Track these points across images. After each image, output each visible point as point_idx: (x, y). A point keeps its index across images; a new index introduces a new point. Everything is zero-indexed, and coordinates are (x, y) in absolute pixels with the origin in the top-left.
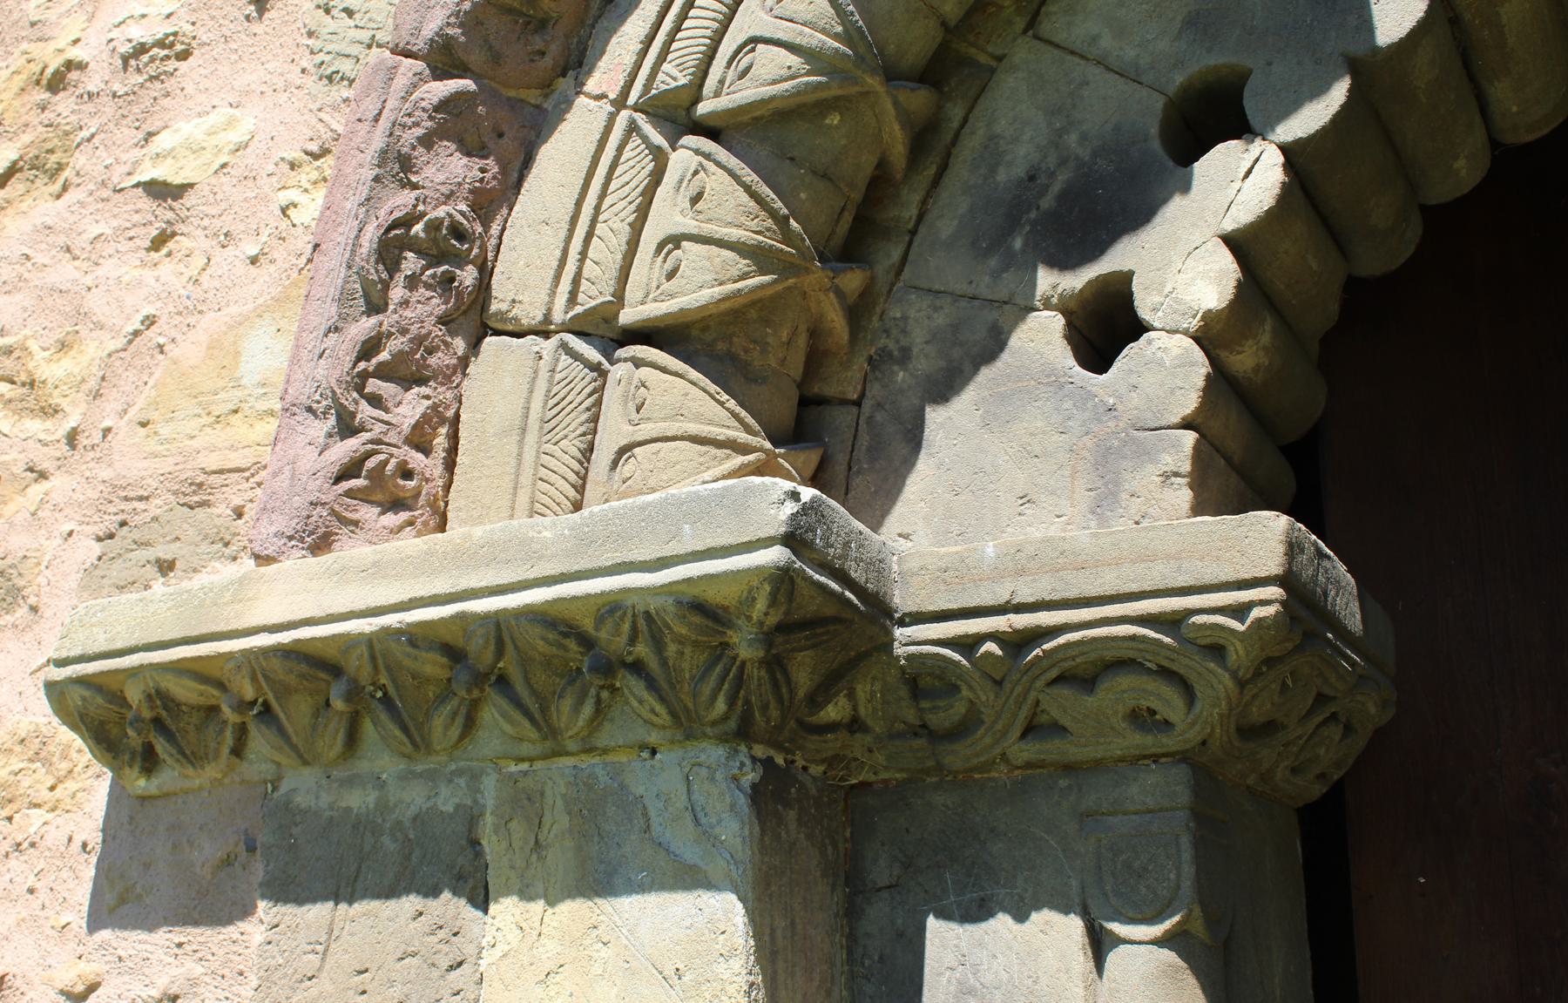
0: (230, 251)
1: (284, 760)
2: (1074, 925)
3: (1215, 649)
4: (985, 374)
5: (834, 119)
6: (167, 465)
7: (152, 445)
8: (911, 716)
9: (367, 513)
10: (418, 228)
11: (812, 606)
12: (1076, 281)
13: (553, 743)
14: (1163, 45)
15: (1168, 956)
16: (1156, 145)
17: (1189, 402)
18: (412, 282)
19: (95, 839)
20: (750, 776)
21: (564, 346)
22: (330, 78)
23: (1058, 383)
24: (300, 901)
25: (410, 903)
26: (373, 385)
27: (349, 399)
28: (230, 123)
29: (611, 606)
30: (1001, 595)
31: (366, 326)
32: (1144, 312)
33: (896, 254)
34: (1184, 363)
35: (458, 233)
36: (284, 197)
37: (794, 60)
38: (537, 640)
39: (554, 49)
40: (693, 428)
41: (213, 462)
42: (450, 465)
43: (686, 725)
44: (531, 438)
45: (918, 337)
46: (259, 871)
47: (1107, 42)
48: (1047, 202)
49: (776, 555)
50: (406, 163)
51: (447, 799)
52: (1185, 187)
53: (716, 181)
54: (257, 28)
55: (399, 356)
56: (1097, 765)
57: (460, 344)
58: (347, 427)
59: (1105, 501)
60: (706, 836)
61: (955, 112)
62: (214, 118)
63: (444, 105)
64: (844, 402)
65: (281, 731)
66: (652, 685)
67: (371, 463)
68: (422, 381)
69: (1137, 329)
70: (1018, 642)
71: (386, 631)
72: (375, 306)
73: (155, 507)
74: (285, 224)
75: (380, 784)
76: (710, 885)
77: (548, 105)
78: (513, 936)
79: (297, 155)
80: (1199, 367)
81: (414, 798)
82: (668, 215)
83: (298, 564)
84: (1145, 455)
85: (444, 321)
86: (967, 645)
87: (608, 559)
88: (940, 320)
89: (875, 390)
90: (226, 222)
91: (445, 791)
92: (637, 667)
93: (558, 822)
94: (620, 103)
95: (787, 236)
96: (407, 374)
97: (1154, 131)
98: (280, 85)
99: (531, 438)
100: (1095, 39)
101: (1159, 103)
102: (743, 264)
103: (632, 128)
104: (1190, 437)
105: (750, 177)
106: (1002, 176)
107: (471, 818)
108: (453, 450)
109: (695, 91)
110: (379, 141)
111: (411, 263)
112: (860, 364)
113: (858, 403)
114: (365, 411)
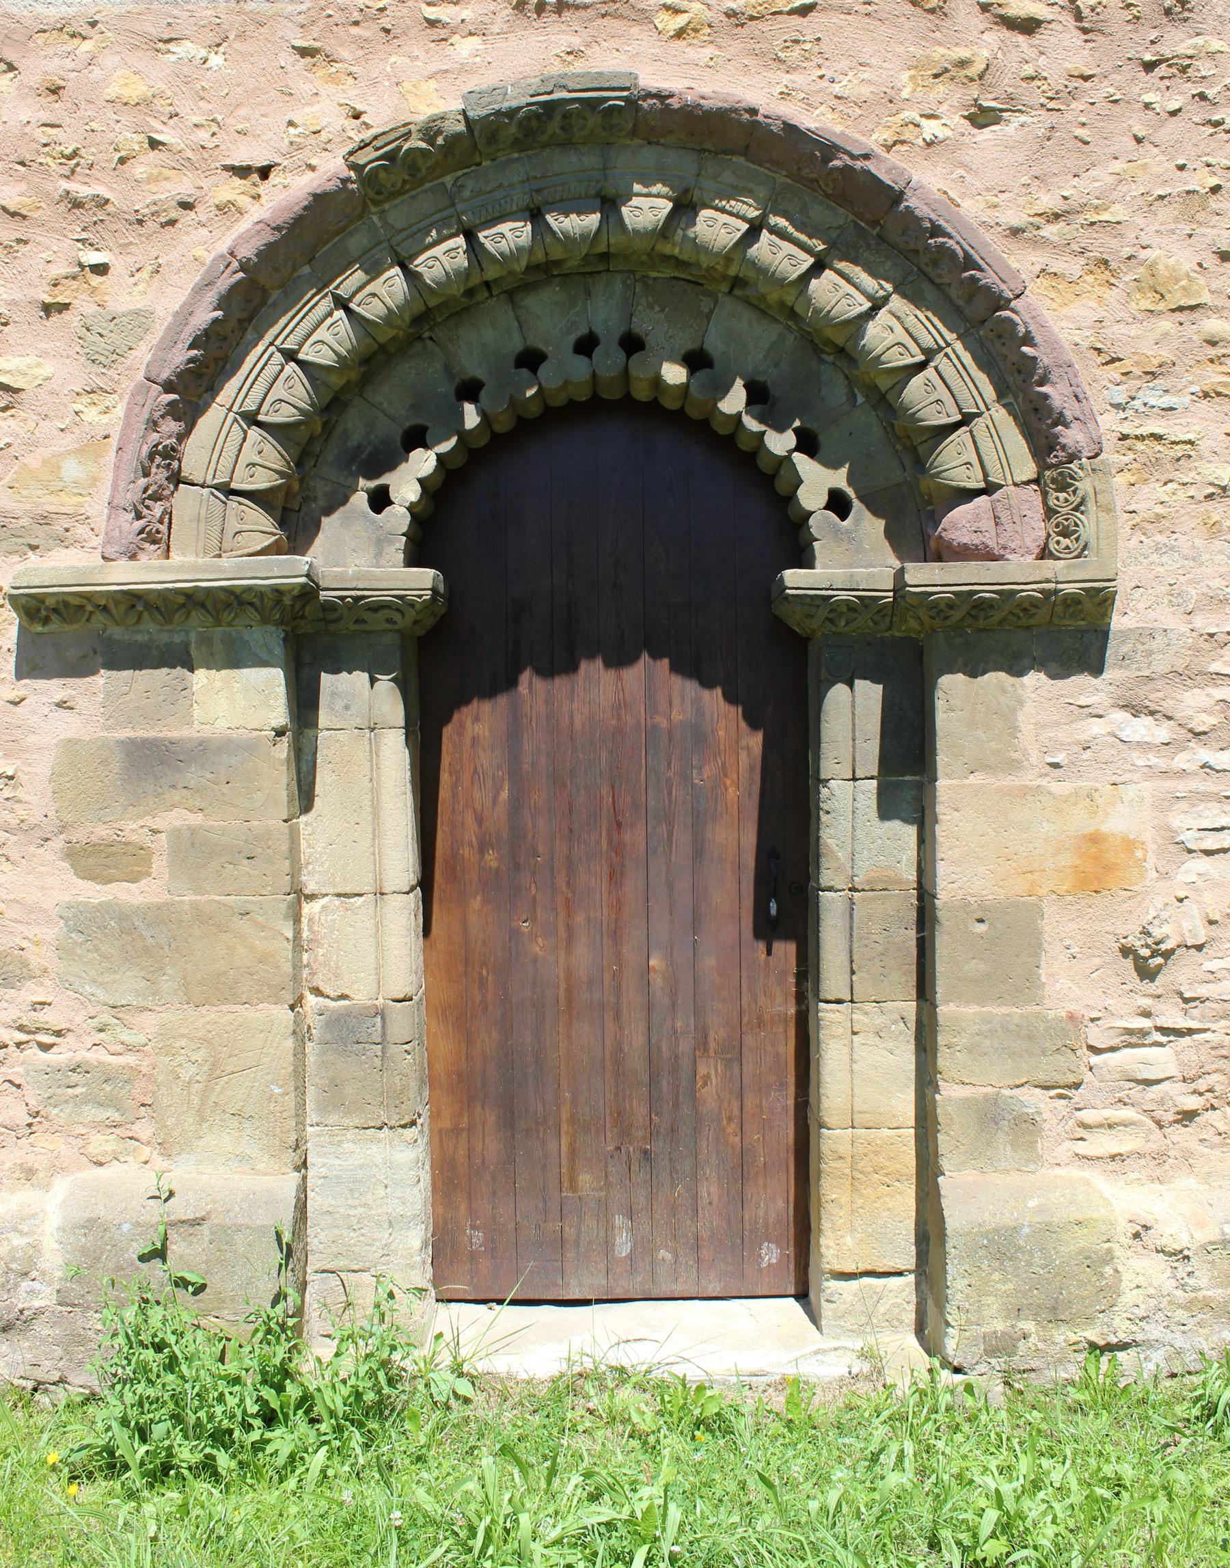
0: (47, 423)
1: (108, 623)
2: (366, 675)
3: (412, 605)
4: (342, 509)
5: (303, 427)
6: (28, 506)
7: (18, 497)
8: (321, 615)
9: (147, 545)
10: (160, 447)
11: (308, 589)
12: (373, 484)
13: (218, 622)
14: (403, 412)
15: (392, 684)
16: (399, 444)
17: (405, 529)
18: (158, 466)
19: (14, 648)
20: (282, 635)
21: (213, 494)
22: (93, 361)
23: (366, 517)
24: (119, 670)
25: (165, 670)
26: (147, 502)
27: (140, 507)
28: (39, 365)
29: (249, 589)
30: (353, 585)
31: (143, 482)
32: (393, 499)
33: (312, 463)
34: (403, 516)
35: (173, 449)
36: (77, 407)
37: (294, 411)
38: (222, 596)
39: (205, 385)
40: (261, 528)
41: (52, 509)
42: (170, 528)
43: (265, 621)
44: (202, 524)
45: (320, 493)
46: (100, 660)
47: (385, 406)
48: (364, 456)
49: (303, 580)
50: (155, 424)
51: (177, 639)
52: (407, 460)
53: (268, 448)
54: (45, 322)
55: (155, 492)
56: (373, 632)
57: (172, 487)
58: (139, 516)
59: (379, 554)
60: (270, 652)
61: (334, 418)
62: (28, 360)
63: (169, 404)
64: (293, 510)
65: (111, 615)
66: (256, 609)
67: (148, 529)
68: (160, 500)
69: (390, 503)
70: (357, 599)
71: (167, 590)
72: (146, 474)
73: (22, 522)
74: (78, 419)
75: (148, 632)
76: (272, 666)
77: (201, 403)
78: (205, 681)
79: (79, 390)
80: (408, 518)
81: (164, 638)
82: (249, 455)
83: (123, 562)
84: (391, 542)
85: (167, 479)
86: (342, 598)
87: (249, 575)
88: (327, 489)
89: (304, 509)
90: (44, 410)
91: (176, 636)
92: (251, 604)
93: (218, 647)
94: (230, 410)
95: (290, 468)
96: (156, 497)
97: (399, 440)
98: (65, 354)
99: (202, 524)
100: (381, 403)
101: (401, 431)
102: (277, 476)
103: (235, 420)
104: (404, 538)
105: (280, 448)
106: (349, 444)
107: (186, 645)
108: (170, 523)
109: (258, 411)
110: (145, 415)
111: (158, 459)
112: (299, 499)
113: (299, 511)
114: (145, 512)
